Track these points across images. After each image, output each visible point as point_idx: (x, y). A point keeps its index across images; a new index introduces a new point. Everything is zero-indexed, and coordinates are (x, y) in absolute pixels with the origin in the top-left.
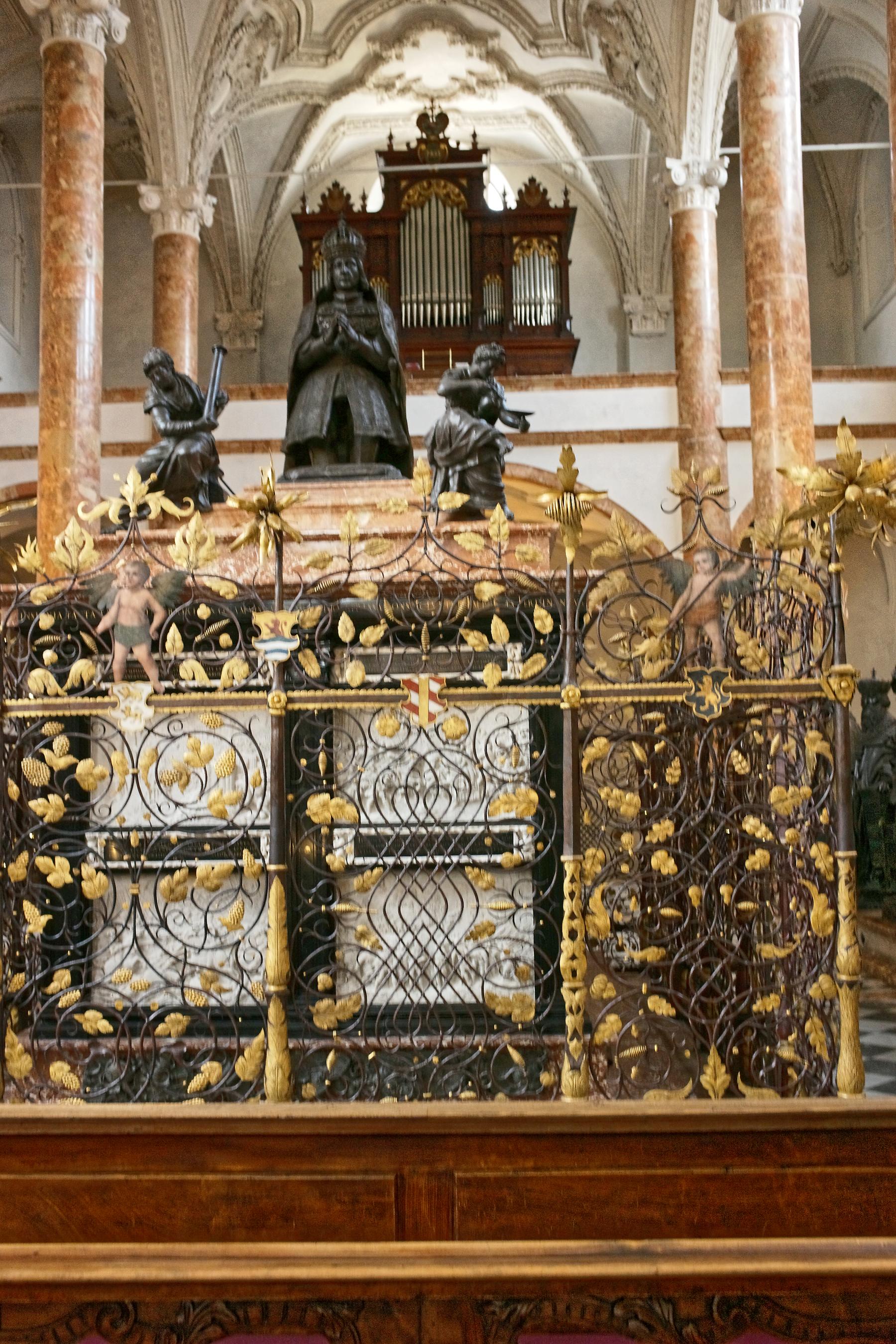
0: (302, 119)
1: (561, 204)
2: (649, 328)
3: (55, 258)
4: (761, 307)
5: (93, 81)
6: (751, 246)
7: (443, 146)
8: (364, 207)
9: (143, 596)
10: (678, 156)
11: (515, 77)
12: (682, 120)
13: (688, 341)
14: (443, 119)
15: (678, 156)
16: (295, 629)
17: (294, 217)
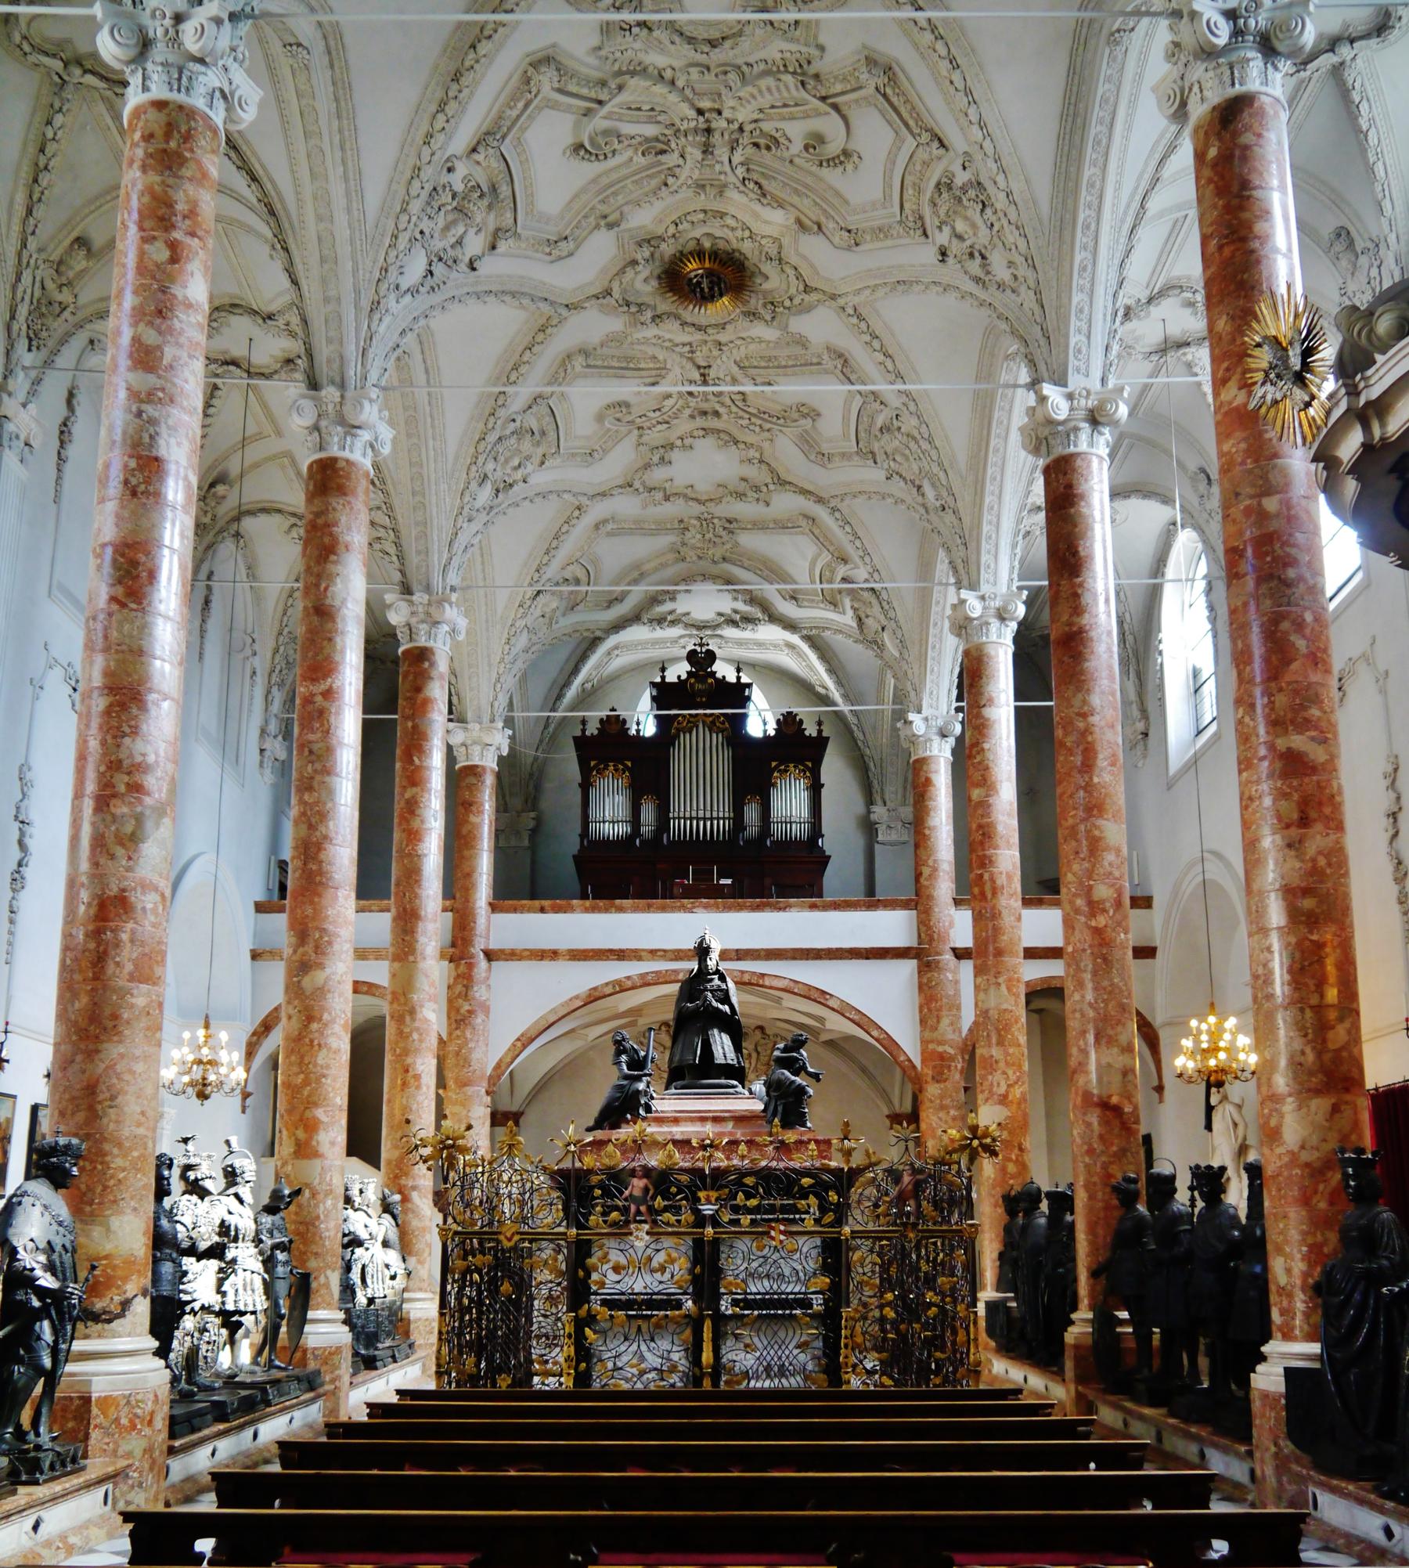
0: (584, 646)
1: (814, 734)
2: (894, 836)
3: (408, 821)
4: (981, 876)
5: (441, 677)
6: (974, 826)
7: (710, 680)
8: (638, 731)
9: (645, 1181)
10: (919, 712)
11: (774, 618)
13: (926, 871)
14: (711, 657)
15: (919, 712)
16: (717, 1199)
17: (575, 739)
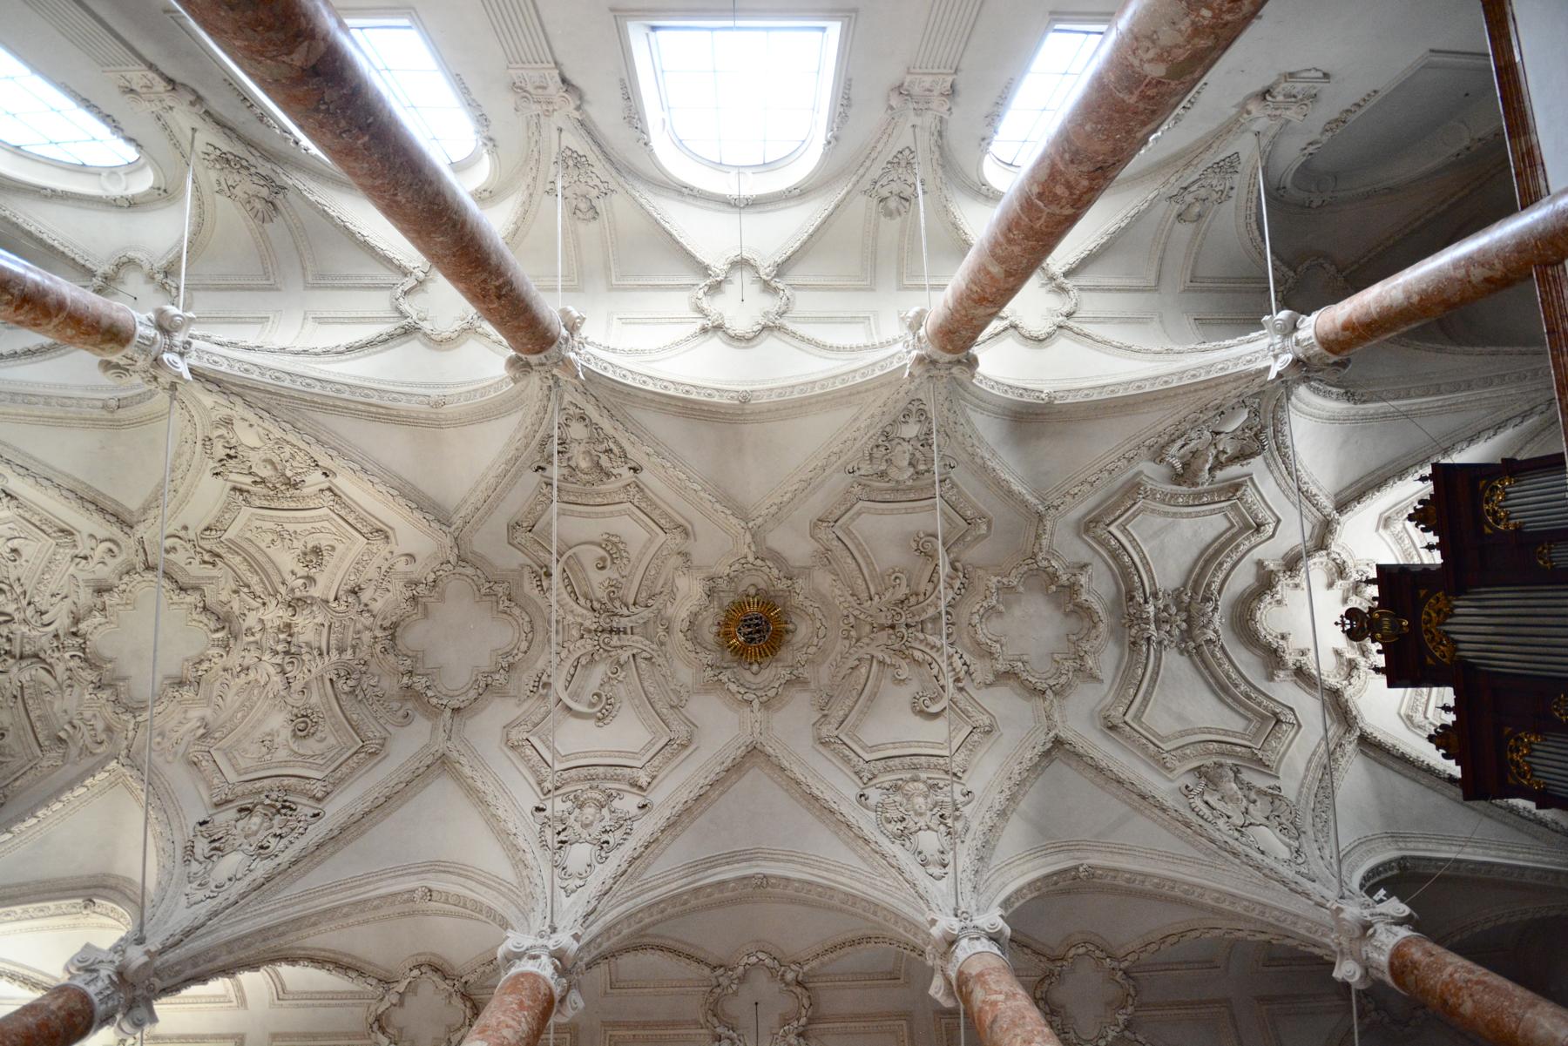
12: (1238, 377)
